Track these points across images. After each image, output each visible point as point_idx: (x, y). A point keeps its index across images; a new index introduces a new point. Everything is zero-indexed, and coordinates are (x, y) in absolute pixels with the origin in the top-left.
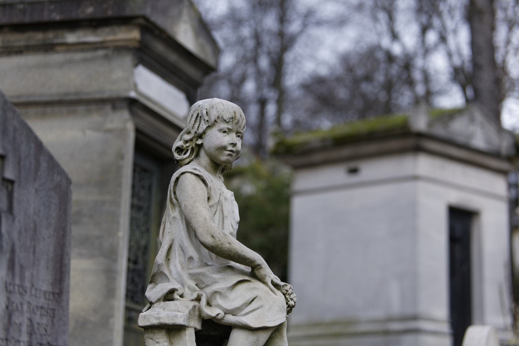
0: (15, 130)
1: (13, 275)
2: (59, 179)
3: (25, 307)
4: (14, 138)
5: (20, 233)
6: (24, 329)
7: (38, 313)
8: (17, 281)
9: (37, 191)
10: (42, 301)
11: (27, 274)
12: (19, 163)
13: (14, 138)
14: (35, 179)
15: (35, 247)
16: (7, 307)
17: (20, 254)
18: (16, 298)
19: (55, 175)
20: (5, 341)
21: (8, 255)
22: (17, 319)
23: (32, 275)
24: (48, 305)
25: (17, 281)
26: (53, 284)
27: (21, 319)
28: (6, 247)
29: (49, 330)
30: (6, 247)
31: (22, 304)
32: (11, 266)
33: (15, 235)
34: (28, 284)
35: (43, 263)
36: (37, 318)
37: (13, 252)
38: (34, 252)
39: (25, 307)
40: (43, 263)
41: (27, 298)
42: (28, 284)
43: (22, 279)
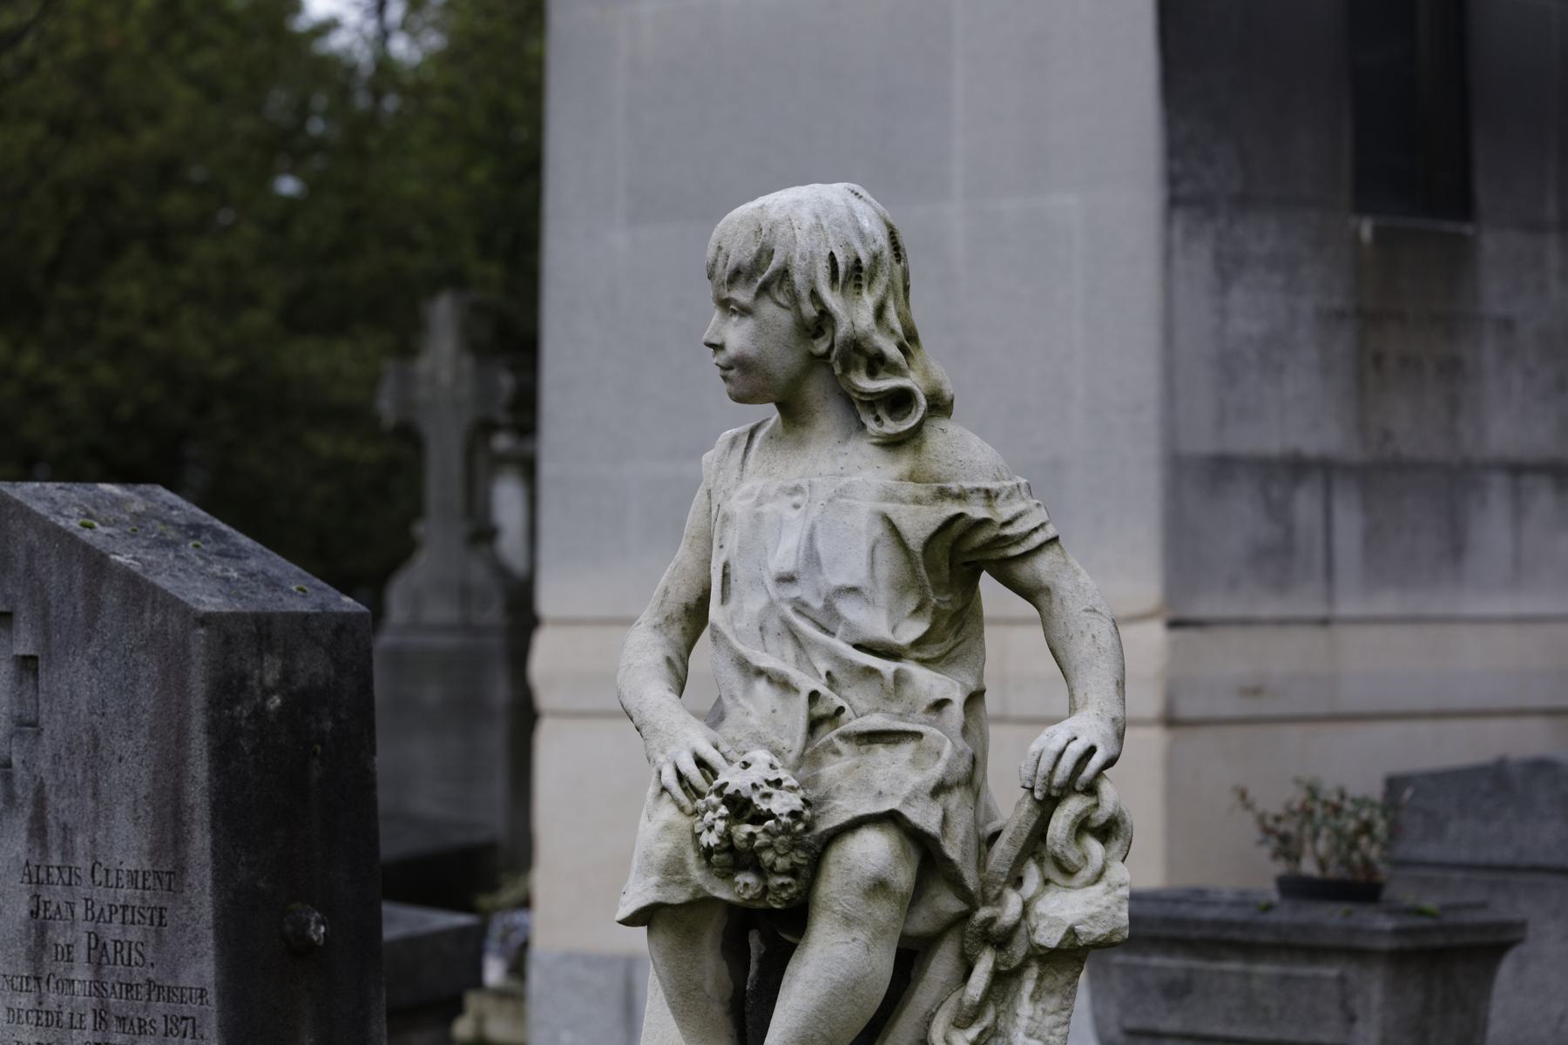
0: (31, 551)
1: (44, 846)
2: (158, 618)
3: (80, 910)
4: (29, 571)
5: (56, 759)
6: (80, 953)
7: (117, 918)
8: (56, 859)
9: (94, 663)
10: (125, 893)
11: (80, 840)
12: (46, 614)
13: (29, 571)
14: (89, 639)
15: (96, 781)
16: (34, 914)
17: (60, 805)
18: (56, 894)
19: (147, 615)
20: (32, 983)
21: (28, 811)
22: (59, 935)
23: (93, 842)
24: (143, 899)
25: (56, 859)
26: (154, 853)
27: (73, 934)
28: (23, 793)
29: (149, 954)
30: (23, 793)
31: (71, 905)
32: (38, 830)
33: (44, 765)
34: (82, 863)
35: (121, 812)
36: (112, 932)
37: (40, 802)
38: (95, 795)
39: (80, 910)
40: (121, 812)
41: (82, 890)
42: (82, 863)
43: (67, 853)
